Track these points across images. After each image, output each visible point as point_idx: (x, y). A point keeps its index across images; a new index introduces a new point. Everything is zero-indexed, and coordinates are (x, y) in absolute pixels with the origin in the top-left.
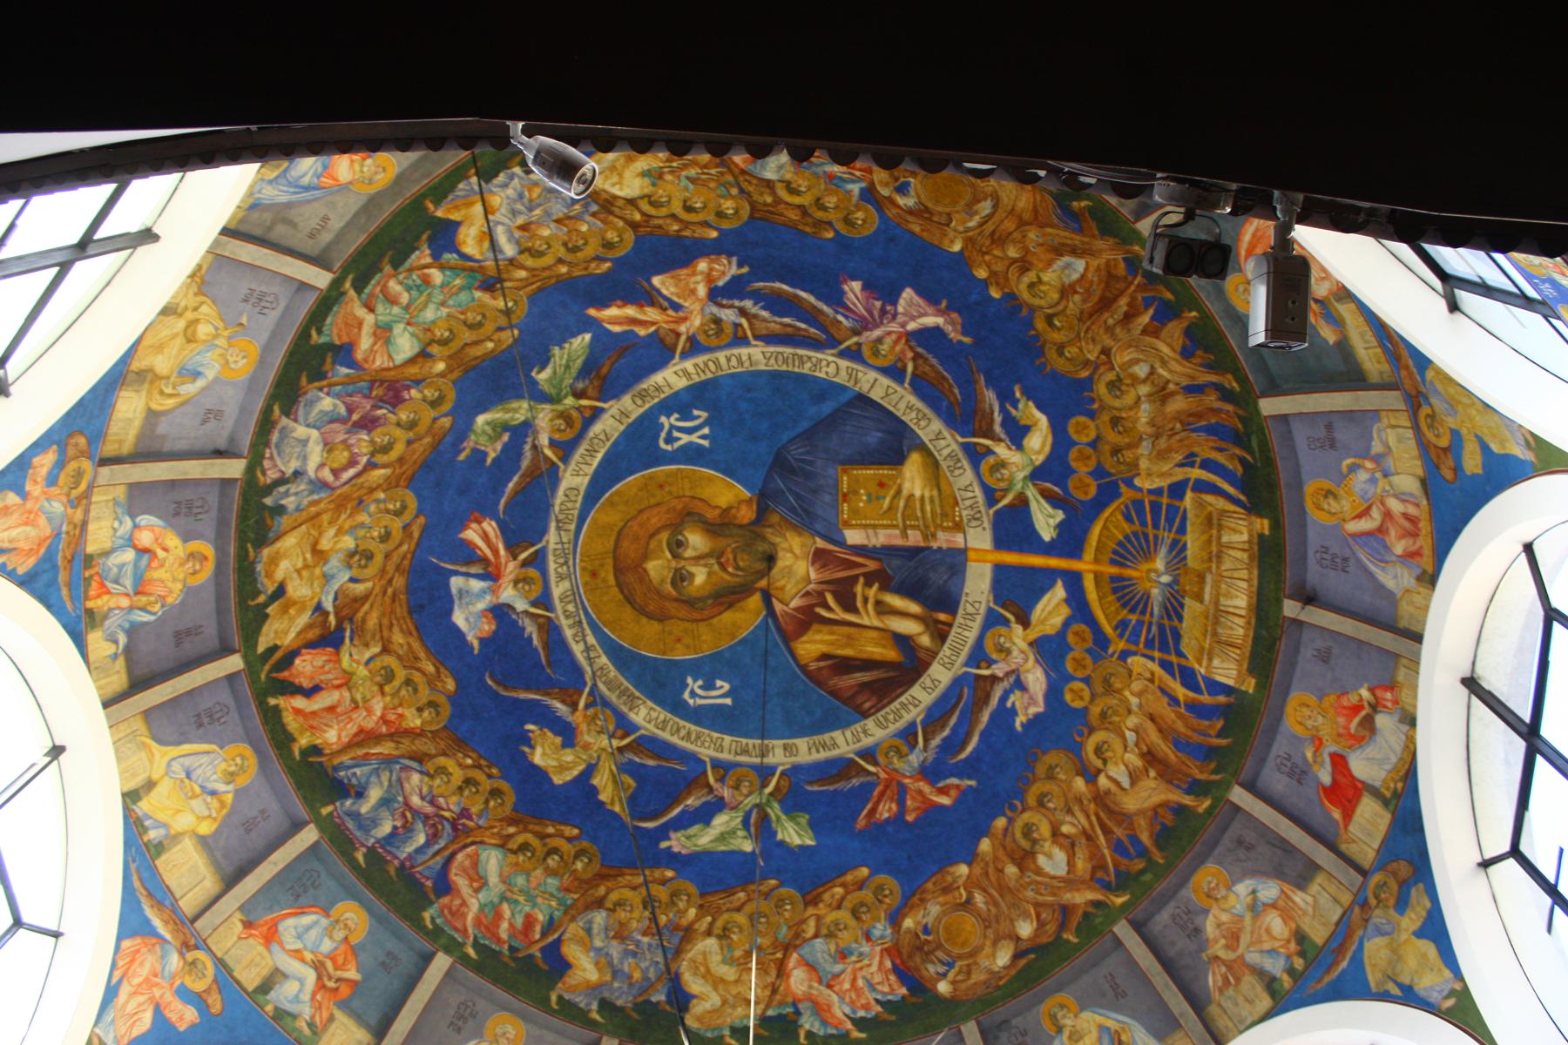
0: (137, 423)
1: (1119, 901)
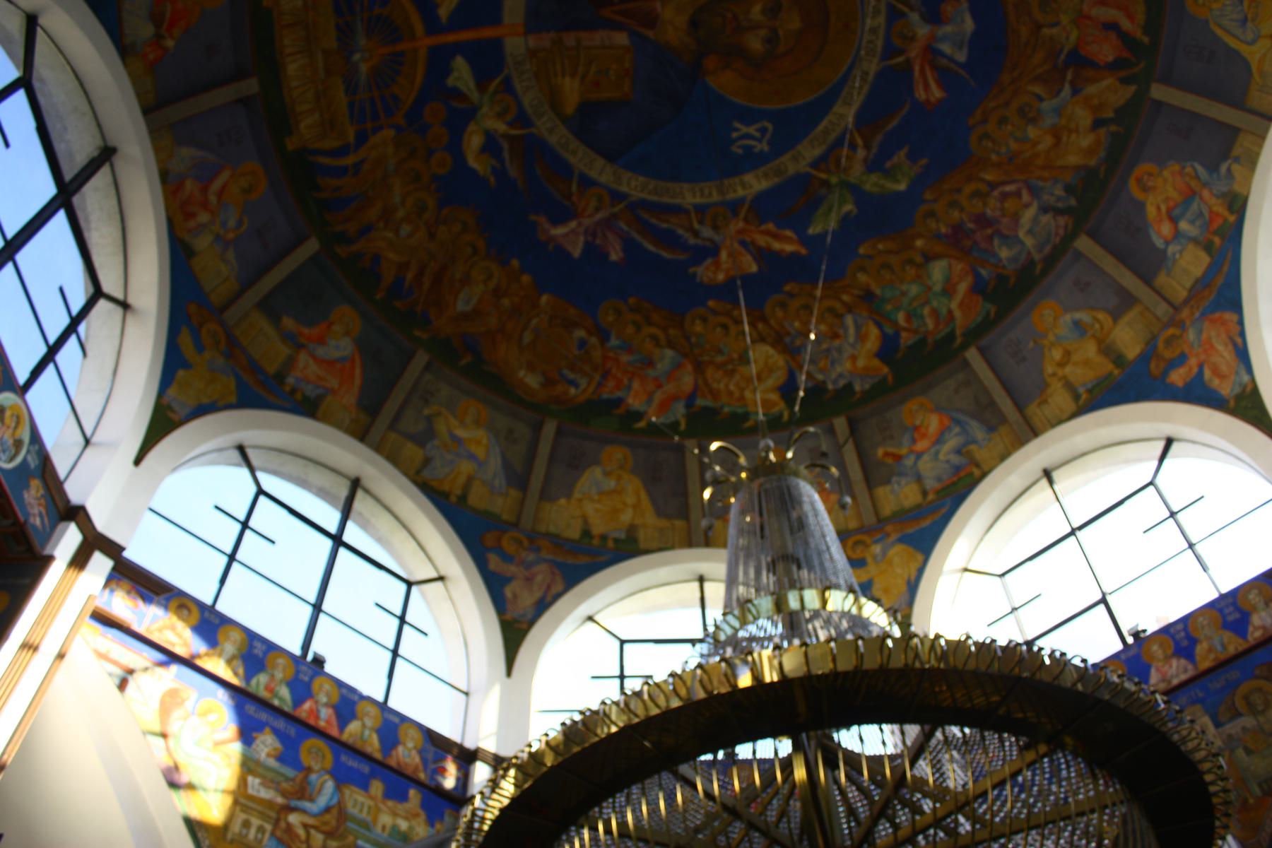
0: (1126, 319)
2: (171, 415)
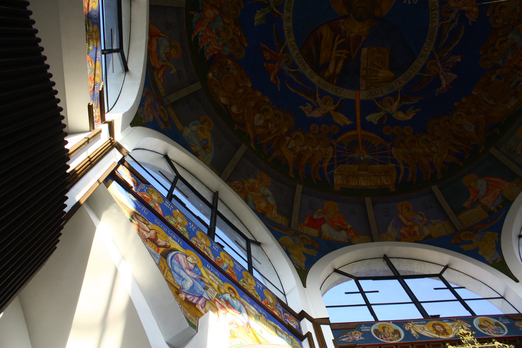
1: (252, 146)
2: (497, 261)
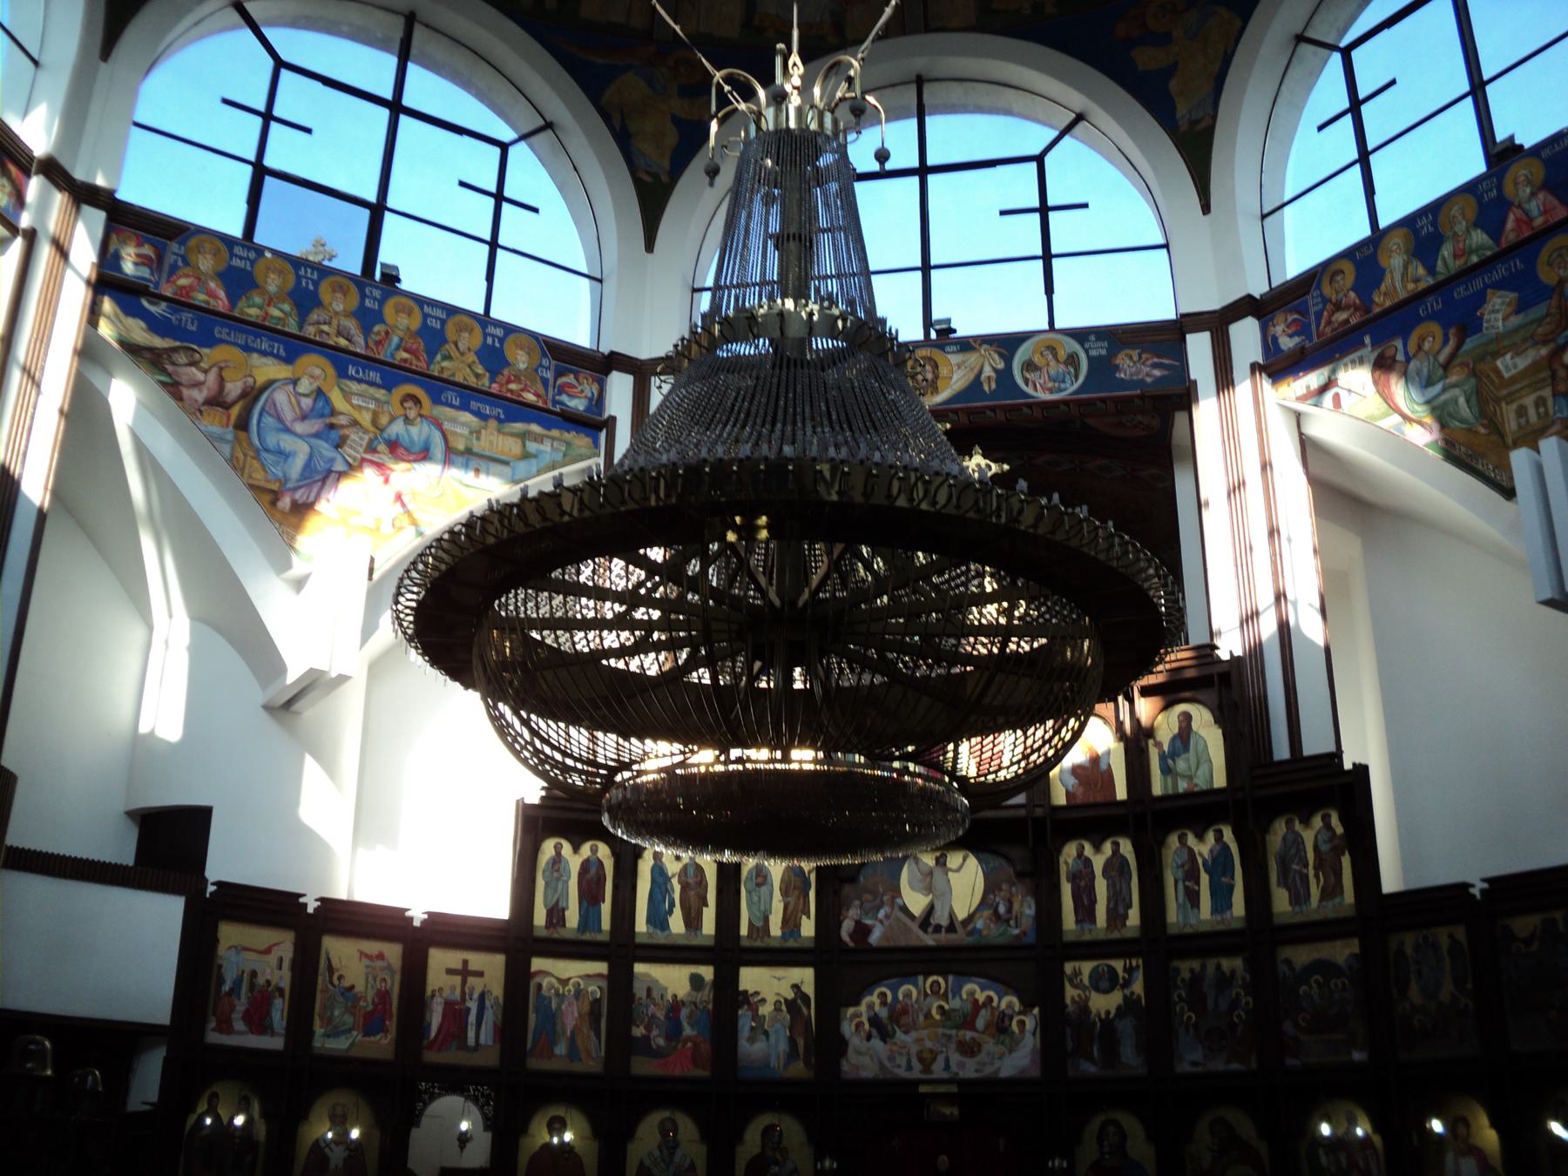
2: (1202, 125)
